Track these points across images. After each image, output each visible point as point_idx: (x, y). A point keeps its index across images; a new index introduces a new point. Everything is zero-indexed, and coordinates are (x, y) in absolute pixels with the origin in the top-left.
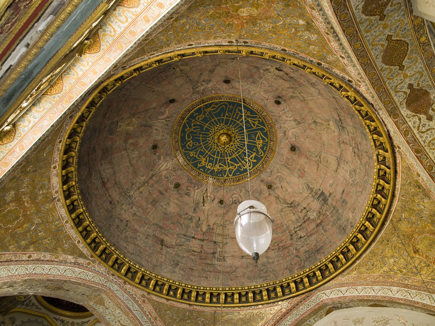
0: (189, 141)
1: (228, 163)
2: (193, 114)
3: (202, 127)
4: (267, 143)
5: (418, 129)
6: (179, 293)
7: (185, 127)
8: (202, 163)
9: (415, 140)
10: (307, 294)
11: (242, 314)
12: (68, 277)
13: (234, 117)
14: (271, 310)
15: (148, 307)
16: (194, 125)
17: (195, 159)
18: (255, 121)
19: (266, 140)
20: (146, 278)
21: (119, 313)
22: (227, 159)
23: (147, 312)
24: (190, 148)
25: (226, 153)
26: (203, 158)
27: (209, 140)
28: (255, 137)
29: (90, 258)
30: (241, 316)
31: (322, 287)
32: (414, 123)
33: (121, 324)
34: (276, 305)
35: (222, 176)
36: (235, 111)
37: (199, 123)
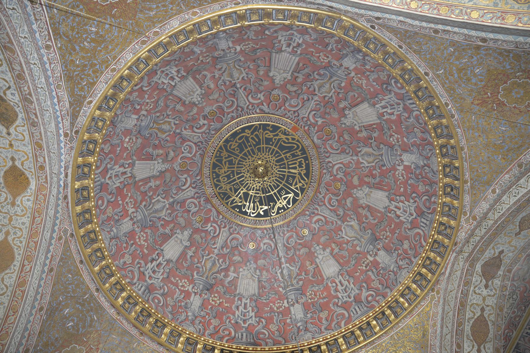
0: (236, 142)
1: (240, 193)
2: (268, 125)
3: (258, 143)
4: (288, 208)
5: (475, 288)
7: (249, 127)
8: (221, 170)
9: (467, 295)
12: (44, 119)
13: (289, 163)
15: (56, 249)
16: (257, 136)
17: (220, 161)
18: (300, 182)
19: (289, 205)
21: (23, 224)
22: (242, 190)
23: (51, 253)
24: (230, 148)
25: (248, 183)
26: (226, 168)
27: (249, 159)
28: (284, 195)
29: (74, 131)
32: (476, 281)
35: (223, 199)
36: (296, 160)
37: (261, 138)
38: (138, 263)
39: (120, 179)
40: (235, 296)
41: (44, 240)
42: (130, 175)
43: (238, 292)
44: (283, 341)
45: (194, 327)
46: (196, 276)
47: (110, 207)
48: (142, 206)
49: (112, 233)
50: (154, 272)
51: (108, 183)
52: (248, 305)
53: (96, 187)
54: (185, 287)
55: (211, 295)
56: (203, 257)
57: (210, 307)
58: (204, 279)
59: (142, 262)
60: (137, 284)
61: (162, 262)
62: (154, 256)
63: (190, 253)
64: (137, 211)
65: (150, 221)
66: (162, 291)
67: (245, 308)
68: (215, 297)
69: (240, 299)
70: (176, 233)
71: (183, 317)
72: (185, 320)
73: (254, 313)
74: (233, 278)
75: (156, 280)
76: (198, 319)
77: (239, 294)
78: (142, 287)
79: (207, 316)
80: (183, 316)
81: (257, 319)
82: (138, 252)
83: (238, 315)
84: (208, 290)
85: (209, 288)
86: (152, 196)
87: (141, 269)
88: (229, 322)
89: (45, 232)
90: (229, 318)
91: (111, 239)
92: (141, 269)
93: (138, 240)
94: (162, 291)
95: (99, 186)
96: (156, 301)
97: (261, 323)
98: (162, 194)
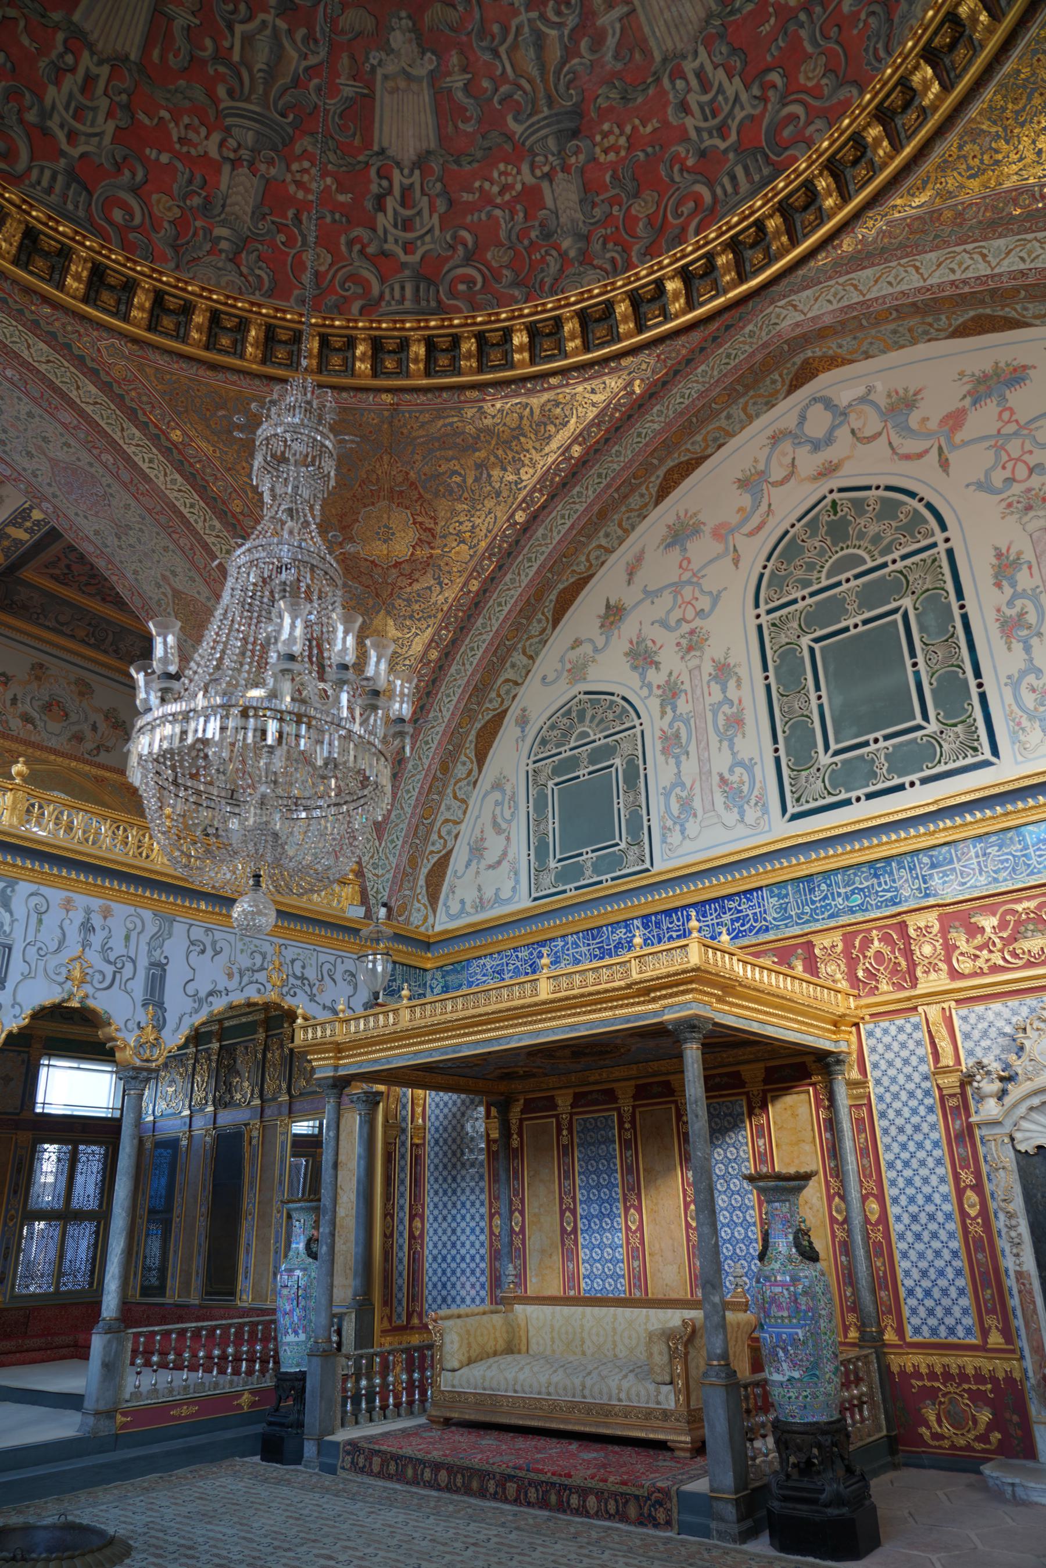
6: (250, 339)
10: (726, 316)
11: (492, 411)
14: (593, 391)
20: (111, 281)
21: (30, 414)
30: (488, 422)
31: (784, 283)
33: (50, 460)
34: (613, 371)
38: (350, 244)
39: (95, 109)
40: (658, 80)
41: (89, 409)
42: (105, 70)
43: (658, 56)
44: (855, 92)
45: (595, 267)
46: (517, 128)
47: (155, 197)
48: (226, 103)
49: (224, 245)
50: (407, 225)
51: (83, 155)
52: (709, 68)
53: (65, 196)
54: (511, 187)
55: (592, 138)
56: (496, 54)
57: (608, 178)
58: (546, 112)
59: (358, 232)
60: (387, 291)
61: (407, 182)
62: (374, 188)
63: (457, 81)
64: (227, 130)
65: (284, 115)
66: (461, 250)
67: (705, 85)
68: (605, 135)
69: (677, 73)
70: (373, 68)
71: (553, 267)
72: (562, 270)
73: (737, 80)
74: (618, 26)
75: (428, 238)
76: (594, 238)
77: (665, 60)
78: (403, 288)
79: (616, 208)
80: (552, 263)
81: (756, 91)
82: (328, 220)
83: (698, 130)
84: (575, 134)
85: (575, 126)
86: (217, 49)
87: (370, 250)
88: (681, 170)
89: (73, 395)
90: (676, 159)
91: (234, 259)
92: (370, 250)
93: (300, 195)
94: (461, 250)
95: (68, 186)
96: (462, 287)
97: (771, 93)
98: (235, 11)
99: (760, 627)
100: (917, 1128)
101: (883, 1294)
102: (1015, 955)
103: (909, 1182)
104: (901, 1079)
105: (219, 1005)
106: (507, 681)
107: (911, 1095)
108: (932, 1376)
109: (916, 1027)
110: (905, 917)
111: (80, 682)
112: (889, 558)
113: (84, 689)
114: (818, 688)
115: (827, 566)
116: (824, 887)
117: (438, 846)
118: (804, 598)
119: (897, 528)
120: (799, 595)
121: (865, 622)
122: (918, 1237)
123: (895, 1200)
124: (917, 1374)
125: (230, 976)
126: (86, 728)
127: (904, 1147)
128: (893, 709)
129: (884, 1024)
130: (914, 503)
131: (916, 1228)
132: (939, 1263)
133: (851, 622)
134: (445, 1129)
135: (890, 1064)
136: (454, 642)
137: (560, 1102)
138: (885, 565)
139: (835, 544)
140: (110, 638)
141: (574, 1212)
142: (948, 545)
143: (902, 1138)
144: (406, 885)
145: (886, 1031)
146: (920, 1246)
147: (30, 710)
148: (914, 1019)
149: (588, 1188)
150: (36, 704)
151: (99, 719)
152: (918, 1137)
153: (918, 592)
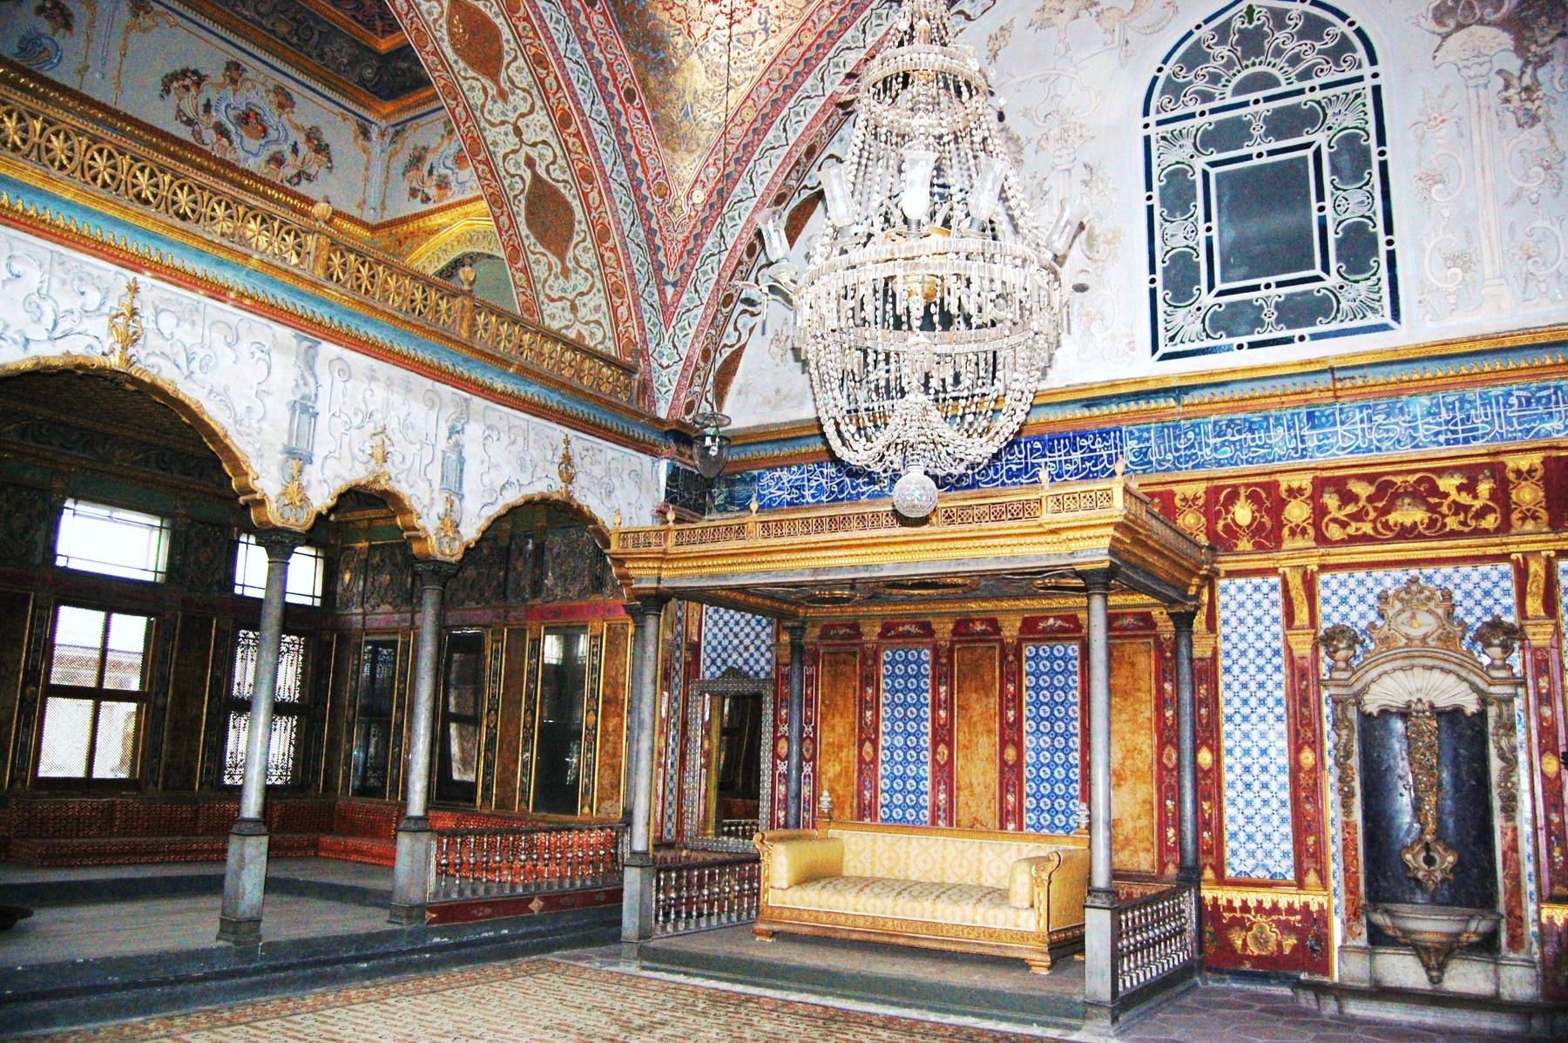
99: (1147, 139)
100: (1261, 685)
101: (1205, 834)
102: (1386, 525)
103: (1246, 736)
104: (1251, 637)
105: (513, 497)
106: (831, 156)
107: (1260, 653)
108: (1245, 908)
109: (1273, 588)
110: (1278, 477)
111: (280, 91)
112: (1307, 84)
113: (285, 101)
114: (1208, 218)
115: (1235, 81)
116: (1191, 435)
117: (733, 340)
118: (1202, 114)
119: (1320, 52)
120: (1198, 108)
121: (1271, 153)
122: (1248, 786)
123: (1230, 752)
124: (1230, 906)
125: (522, 468)
126: (286, 148)
127: (1245, 702)
128: (1291, 252)
129: (1240, 581)
130: (1342, 27)
131: (1248, 778)
132: (1266, 811)
133: (1254, 150)
134: (725, 649)
135: (1241, 621)
136: (776, 104)
137: (865, 629)
138: (1301, 92)
139: (1246, 56)
140: (316, 37)
141: (875, 743)
142: (1376, 82)
143: (1245, 694)
144: (697, 381)
145: (1241, 589)
146: (1248, 795)
147: (224, 120)
148: (1275, 580)
149: (893, 720)
150: (231, 113)
151: (301, 138)
152: (1262, 694)
153: (1336, 128)
